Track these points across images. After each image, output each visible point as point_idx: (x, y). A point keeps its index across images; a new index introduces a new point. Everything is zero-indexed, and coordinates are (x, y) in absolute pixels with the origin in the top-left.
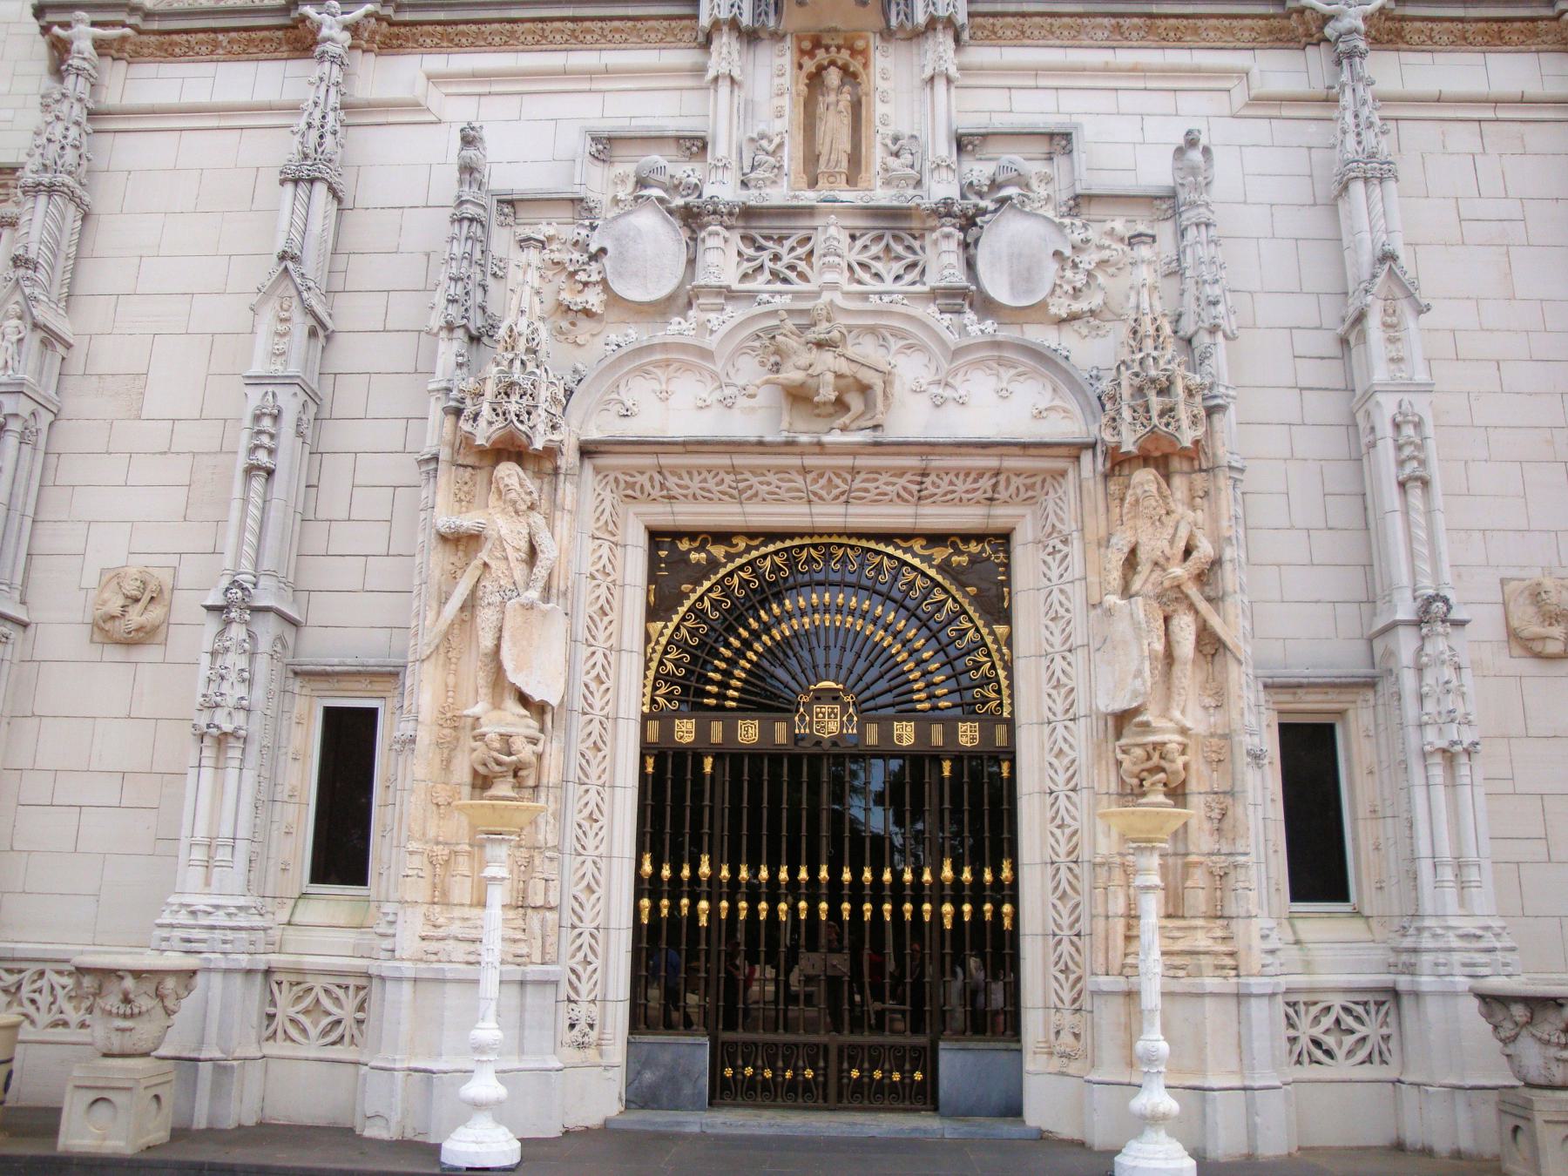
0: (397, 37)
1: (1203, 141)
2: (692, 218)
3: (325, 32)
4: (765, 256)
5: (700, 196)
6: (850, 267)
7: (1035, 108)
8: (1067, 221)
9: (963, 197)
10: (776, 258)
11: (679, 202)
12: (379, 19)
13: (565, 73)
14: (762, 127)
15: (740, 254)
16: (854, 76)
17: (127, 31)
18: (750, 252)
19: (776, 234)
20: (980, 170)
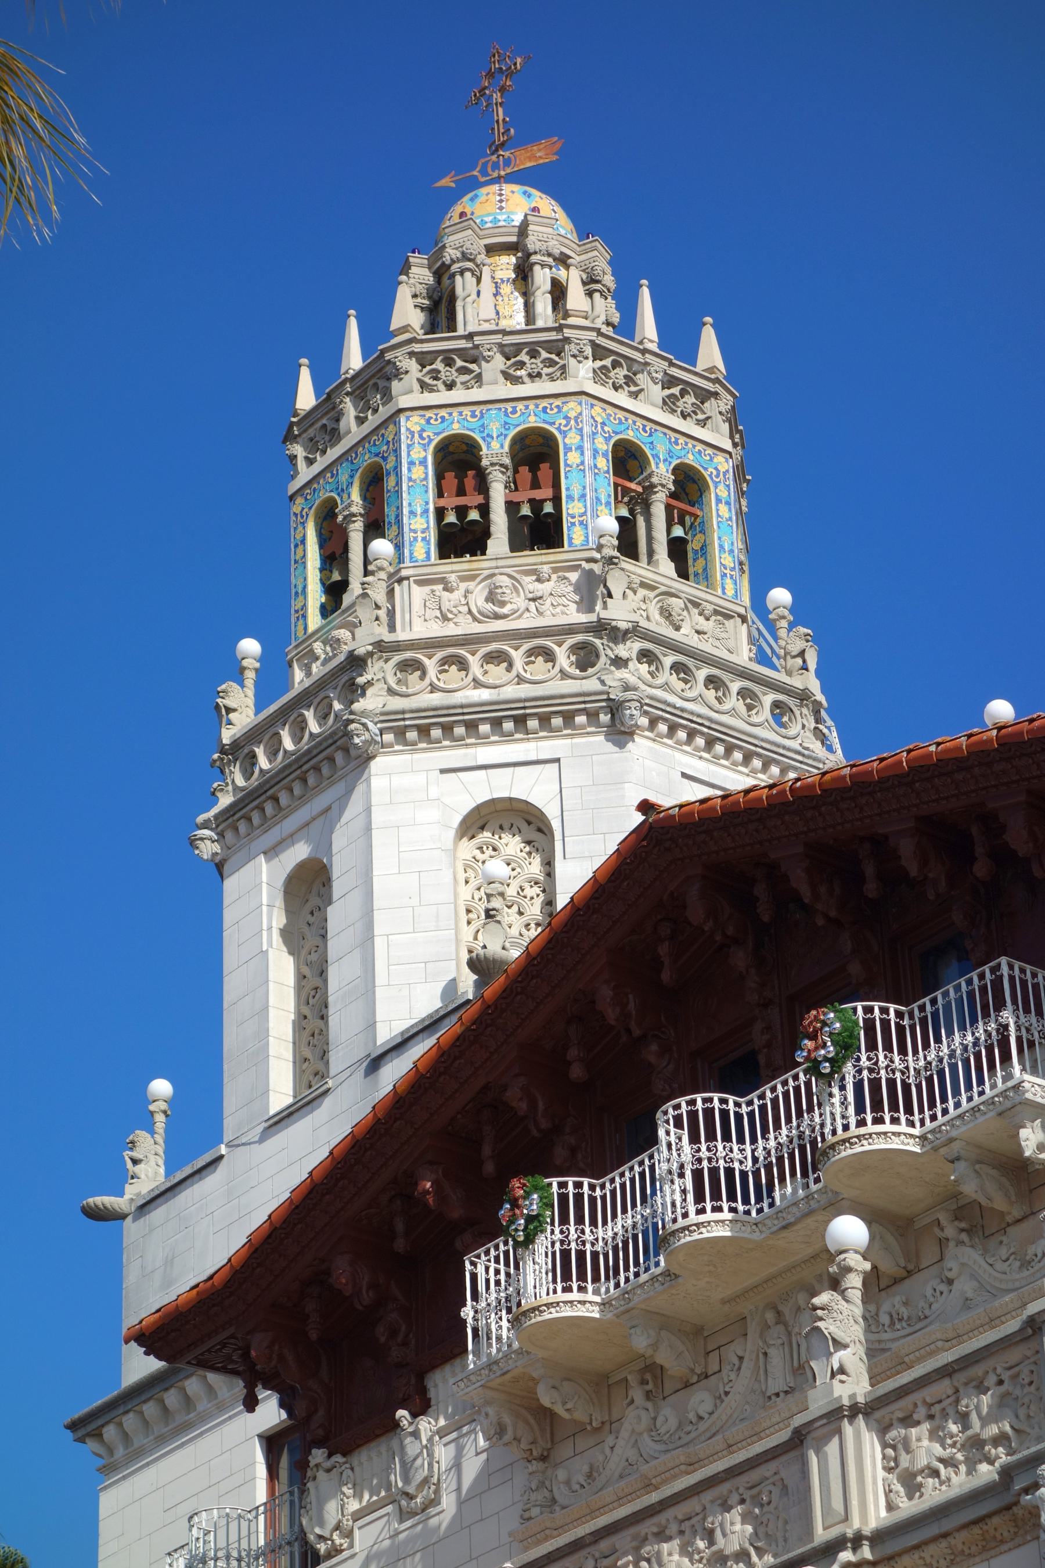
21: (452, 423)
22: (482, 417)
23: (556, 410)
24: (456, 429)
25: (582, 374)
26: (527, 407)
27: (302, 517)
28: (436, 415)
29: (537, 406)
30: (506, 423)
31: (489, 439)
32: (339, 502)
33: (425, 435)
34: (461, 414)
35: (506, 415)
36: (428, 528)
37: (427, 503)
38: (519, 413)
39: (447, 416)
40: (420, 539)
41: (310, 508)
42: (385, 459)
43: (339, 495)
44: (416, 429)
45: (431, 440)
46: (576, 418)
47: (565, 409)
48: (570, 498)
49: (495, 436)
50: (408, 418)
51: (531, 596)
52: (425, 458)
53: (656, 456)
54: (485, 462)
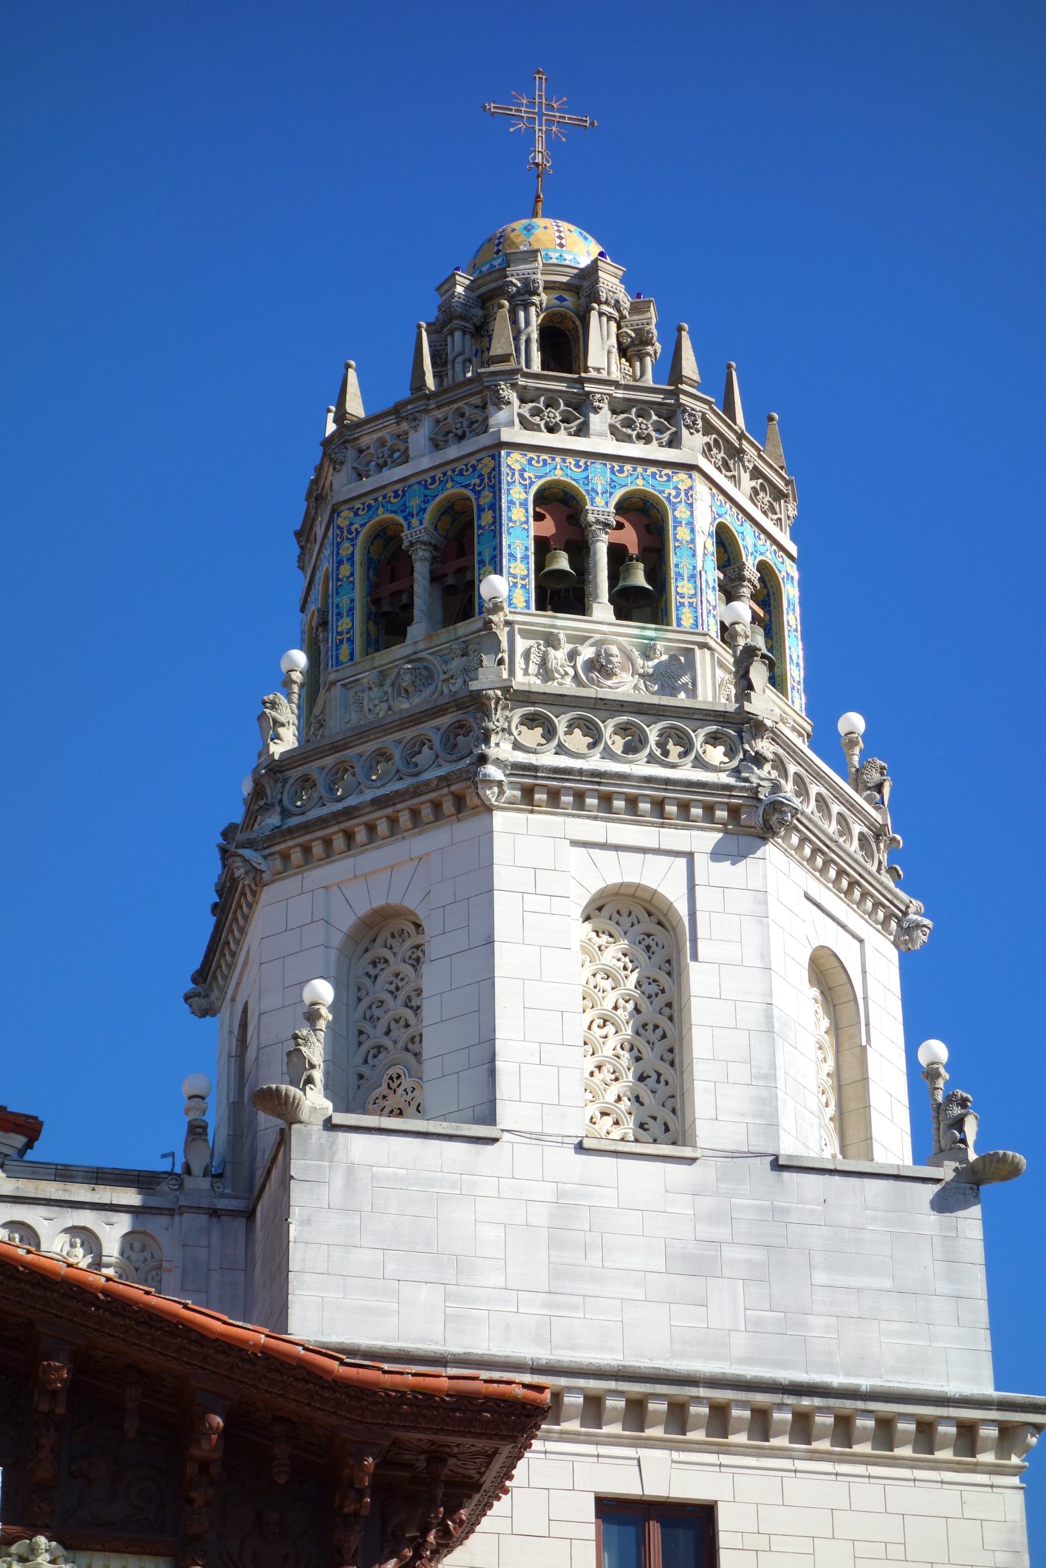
21: (555, 468)
22: (586, 469)
23: (665, 478)
24: (558, 475)
25: (693, 446)
26: (635, 469)
27: (350, 532)
28: (539, 457)
29: (645, 470)
30: (612, 481)
31: (593, 494)
32: (405, 524)
33: (526, 475)
34: (564, 461)
35: (613, 472)
36: (528, 576)
37: (527, 549)
38: (625, 474)
39: (549, 461)
40: (519, 586)
41: (363, 525)
42: (478, 494)
43: (405, 518)
44: (517, 467)
45: (532, 483)
46: (687, 492)
47: (675, 479)
48: (679, 575)
49: (600, 491)
50: (508, 455)
51: (641, 671)
52: (526, 500)
53: (745, 547)
54: (591, 518)
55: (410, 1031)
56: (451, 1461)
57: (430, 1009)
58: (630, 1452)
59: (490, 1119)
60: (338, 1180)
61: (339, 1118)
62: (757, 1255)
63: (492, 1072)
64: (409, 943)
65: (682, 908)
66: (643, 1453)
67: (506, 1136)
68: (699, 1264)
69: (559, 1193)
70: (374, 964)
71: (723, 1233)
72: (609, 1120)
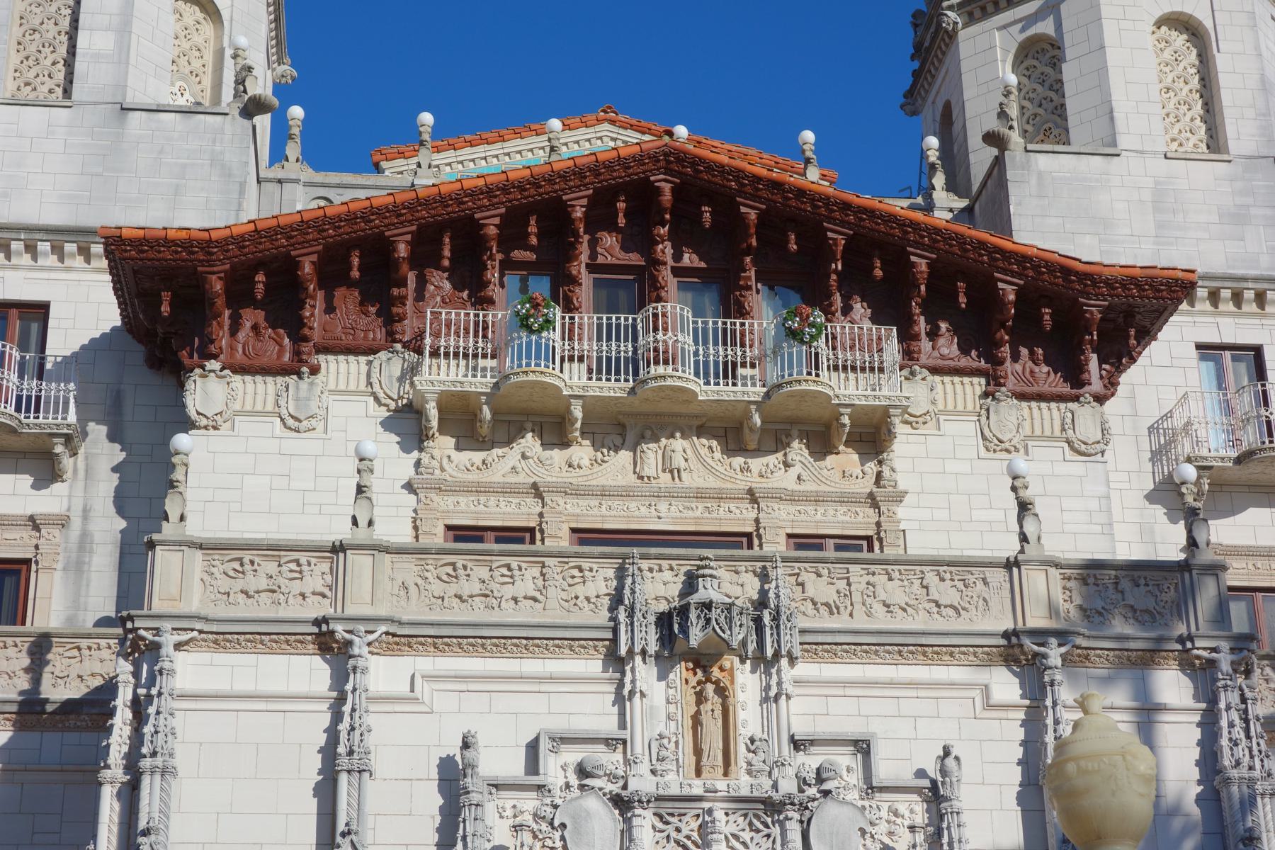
0: (397, 644)
1: (954, 752)
2: (623, 804)
3: (356, 651)
4: (670, 830)
5: (625, 787)
6: (726, 837)
7: (843, 717)
8: (866, 803)
9: (801, 791)
10: (678, 830)
11: (615, 788)
12: (387, 633)
13: (521, 678)
14: (660, 728)
15: (654, 827)
16: (724, 689)
17: (195, 634)
18: (660, 825)
19: (676, 812)
20: (810, 761)
55: (1054, 104)
56: (1138, 317)
57: (1069, 89)
58: (1211, 319)
59: (1114, 144)
60: (1034, 181)
61: (1030, 147)
62: (1269, 212)
63: (1112, 119)
64: (1048, 55)
65: (1208, 24)
66: (1219, 319)
67: (1124, 153)
68: (1238, 218)
69: (1156, 183)
70: (1028, 69)
71: (1250, 200)
72: (1175, 144)
